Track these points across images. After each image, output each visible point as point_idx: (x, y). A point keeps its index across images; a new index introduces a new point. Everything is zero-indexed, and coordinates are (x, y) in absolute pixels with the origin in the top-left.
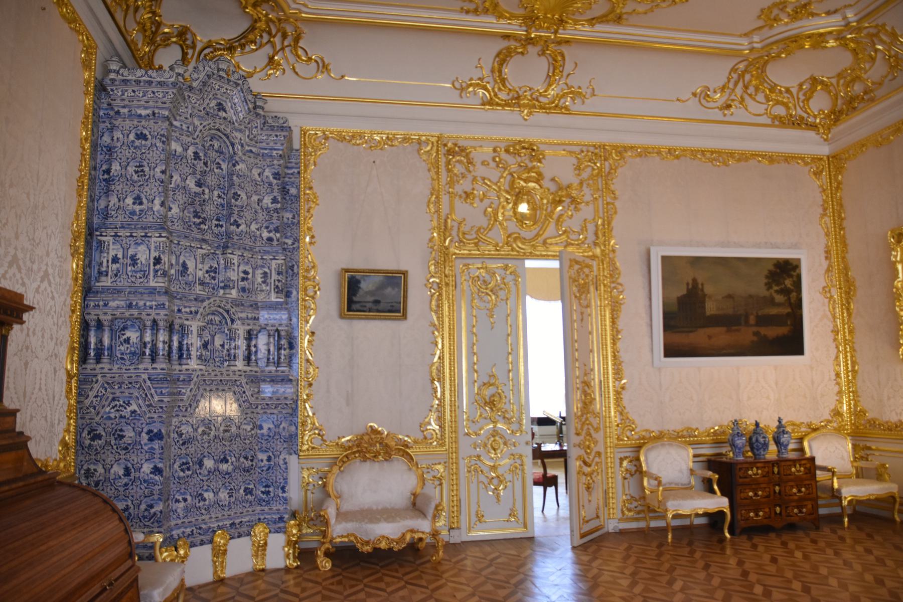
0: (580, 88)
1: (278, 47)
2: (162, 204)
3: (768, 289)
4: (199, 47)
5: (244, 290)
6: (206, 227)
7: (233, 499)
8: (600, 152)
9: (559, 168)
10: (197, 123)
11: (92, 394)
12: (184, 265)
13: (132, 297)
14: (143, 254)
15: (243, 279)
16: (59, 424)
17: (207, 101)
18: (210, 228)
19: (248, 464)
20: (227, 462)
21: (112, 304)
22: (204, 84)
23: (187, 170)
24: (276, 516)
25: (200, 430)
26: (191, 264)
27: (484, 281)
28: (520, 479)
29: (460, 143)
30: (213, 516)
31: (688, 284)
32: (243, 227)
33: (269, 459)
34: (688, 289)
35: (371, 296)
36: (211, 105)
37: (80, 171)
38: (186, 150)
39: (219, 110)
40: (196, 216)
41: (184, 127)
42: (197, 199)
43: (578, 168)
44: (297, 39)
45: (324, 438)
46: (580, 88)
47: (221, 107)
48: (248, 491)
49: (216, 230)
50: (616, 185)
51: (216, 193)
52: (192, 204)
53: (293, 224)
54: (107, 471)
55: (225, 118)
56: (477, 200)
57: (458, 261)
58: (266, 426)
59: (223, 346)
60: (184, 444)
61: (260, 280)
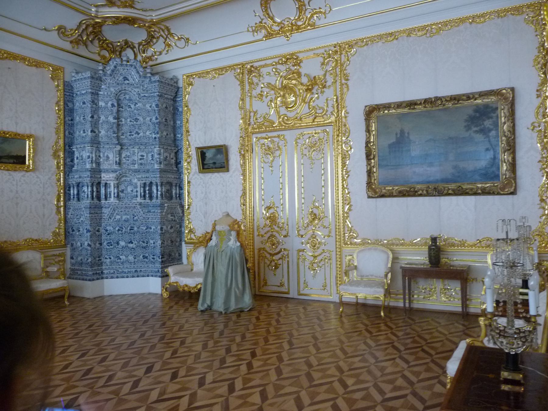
0: (320, 8)
1: (165, 37)
2: (92, 131)
3: (467, 131)
4: (137, 46)
5: (141, 164)
6: (124, 137)
7: (136, 260)
8: (340, 49)
9: (311, 68)
10: (112, 89)
11: (70, 213)
12: (108, 157)
13: (81, 173)
14: (85, 154)
15: (141, 159)
16: (50, 224)
17: (117, 78)
18: (126, 137)
19: (145, 245)
20: (132, 243)
21: (75, 177)
22: (113, 71)
23: (108, 113)
24: (157, 270)
25: (117, 229)
26: (111, 156)
27: (268, 146)
28: (286, 263)
29: (256, 64)
30: (125, 266)
31: (396, 134)
32: (141, 134)
33: (154, 243)
34: (397, 138)
35: (213, 160)
36: (120, 79)
37: (57, 124)
38: (107, 104)
39: (125, 80)
40: (114, 133)
41: (106, 94)
42: (115, 125)
43: (323, 64)
44: (169, 30)
45: (196, 234)
46: (320, 8)
47: (125, 79)
48: (145, 257)
49: (130, 137)
50: (349, 70)
51: (129, 120)
52: (112, 128)
53: (181, 126)
54: (76, 244)
55: (128, 84)
56: (264, 97)
57: (254, 136)
58: (153, 227)
59: (132, 191)
60: (108, 234)
61: (151, 158)
